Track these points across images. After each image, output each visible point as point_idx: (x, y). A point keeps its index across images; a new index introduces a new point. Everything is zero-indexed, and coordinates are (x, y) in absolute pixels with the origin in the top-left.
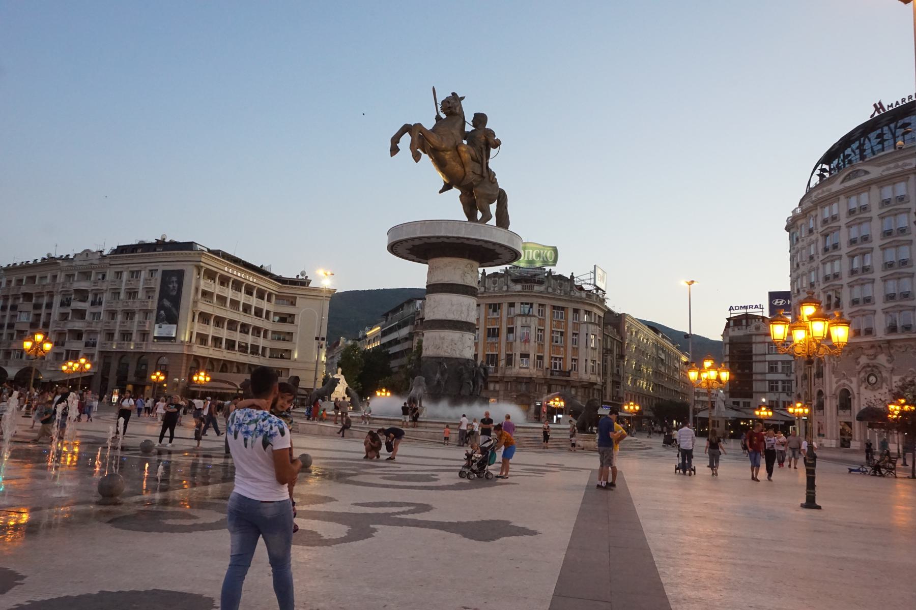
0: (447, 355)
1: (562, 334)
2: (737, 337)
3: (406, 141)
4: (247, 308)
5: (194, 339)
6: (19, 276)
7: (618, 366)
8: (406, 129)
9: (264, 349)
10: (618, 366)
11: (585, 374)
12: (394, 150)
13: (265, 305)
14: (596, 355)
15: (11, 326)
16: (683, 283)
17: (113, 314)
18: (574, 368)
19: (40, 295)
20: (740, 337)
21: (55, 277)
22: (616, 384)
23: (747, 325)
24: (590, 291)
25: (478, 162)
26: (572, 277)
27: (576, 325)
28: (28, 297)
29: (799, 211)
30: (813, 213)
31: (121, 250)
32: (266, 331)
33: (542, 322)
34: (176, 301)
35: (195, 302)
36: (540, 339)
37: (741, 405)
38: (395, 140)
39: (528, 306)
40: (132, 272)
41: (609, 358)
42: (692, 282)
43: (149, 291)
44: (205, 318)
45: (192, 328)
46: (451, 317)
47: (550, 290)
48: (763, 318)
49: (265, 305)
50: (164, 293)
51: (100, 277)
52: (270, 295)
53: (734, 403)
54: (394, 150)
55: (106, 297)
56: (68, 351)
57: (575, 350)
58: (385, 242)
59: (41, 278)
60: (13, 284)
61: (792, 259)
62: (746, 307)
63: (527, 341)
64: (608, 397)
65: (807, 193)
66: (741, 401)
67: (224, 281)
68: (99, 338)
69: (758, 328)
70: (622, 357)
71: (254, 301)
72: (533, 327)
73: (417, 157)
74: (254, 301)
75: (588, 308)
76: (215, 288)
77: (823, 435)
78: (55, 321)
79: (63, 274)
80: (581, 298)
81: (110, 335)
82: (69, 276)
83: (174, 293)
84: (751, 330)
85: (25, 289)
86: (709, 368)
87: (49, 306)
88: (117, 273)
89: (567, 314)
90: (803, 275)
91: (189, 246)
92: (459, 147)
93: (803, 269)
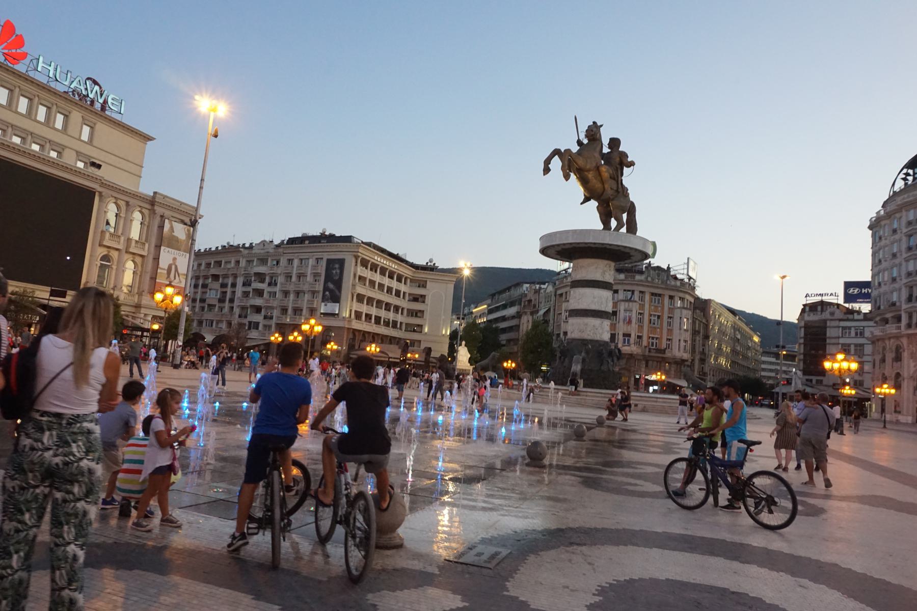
0: (589, 338)
1: (659, 317)
2: (812, 322)
3: (556, 163)
4: (390, 290)
5: (353, 316)
6: (208, 261)
7: (704, 345)
8: (556, 152)
9: (401, 323)
10: (704, 345)
11: (679, 352)
12: (547, 170)
13: (403, 288)
14: (688, 336)
15: (203, 301)
16: (777, 277)
17: (286, 293)
18: (668, 346)
19: (226, 276)
20: (815, 322)
21: (238, 262)
22: (703, 361)
23: (822, 311)
24: (682, 280)
25: (614, 179)
26: (669, 268)
27: (671, 310)
28: (216, 277)
29: (882, 213)
30: (898, 215)
31: (292, 241)
32: (403, 309)
33: (642, 307)
34: (339, 284)
35: (354, 286)
36: (640, 321)
37: (814, 382)
38: (547, 162)
39: (630, 293)
40: (301, 260)
41: (698, 338)
42: (784, 277)
43: (316, 275)
44: (360, 298)
45: (351, 306)
46: (593, 307)
47: (649, 279)
48: (838, 305)
49: (403, 288)
50: (328, 277)
51: (275, 263)
52: (406, 278)
53: (807, 380)
54: (547, 170)
55: (280, 280)
56: (250, 323)
57: (670, 331)
58: (537, 246)
59: (226, 262)
60: (203, 267)
61: (874, 255)
62: (821, 295)
63: (630, 322)
65: (890, 198)
66: (814, 378)
67: (374, 268)
68: (276, 313)
69: (832, 314)
70: (706, 337)
71: (394, 284)
72: (634, 312)
73: (567, 177)
74: (394, 284)
75: (682, 295)
76: (368, 274)
77: (900, 412)
78: (238, 298)
79: (244, 261)
80: (676, 286)
81: (284, 310)
82: (249, 262)
83: (337, 278)
84: (826, 315)
85: (213, 271)
86: (842, 360)
87: (234, 285)
88: (289, 260)
89: (663, 301)
90: (884, 270)
91: (348, 239)
92: (598, 167)
93: (884, 264)
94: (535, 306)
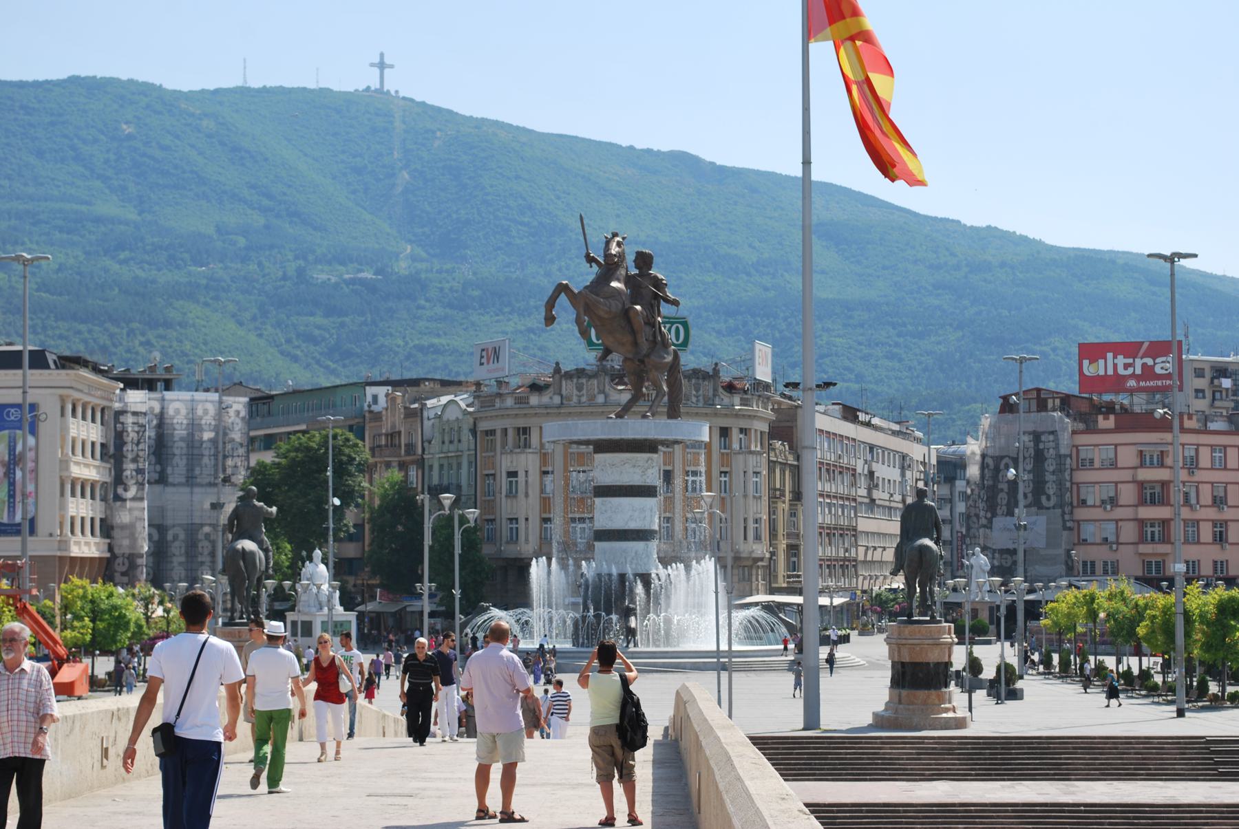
7: (793, 514)
12: (550, 319)
38: (551, 304)
45: (63, 507)
46: (633, 525)
54: (550, 319)
64: (780, 579)
94: (410, 448)
